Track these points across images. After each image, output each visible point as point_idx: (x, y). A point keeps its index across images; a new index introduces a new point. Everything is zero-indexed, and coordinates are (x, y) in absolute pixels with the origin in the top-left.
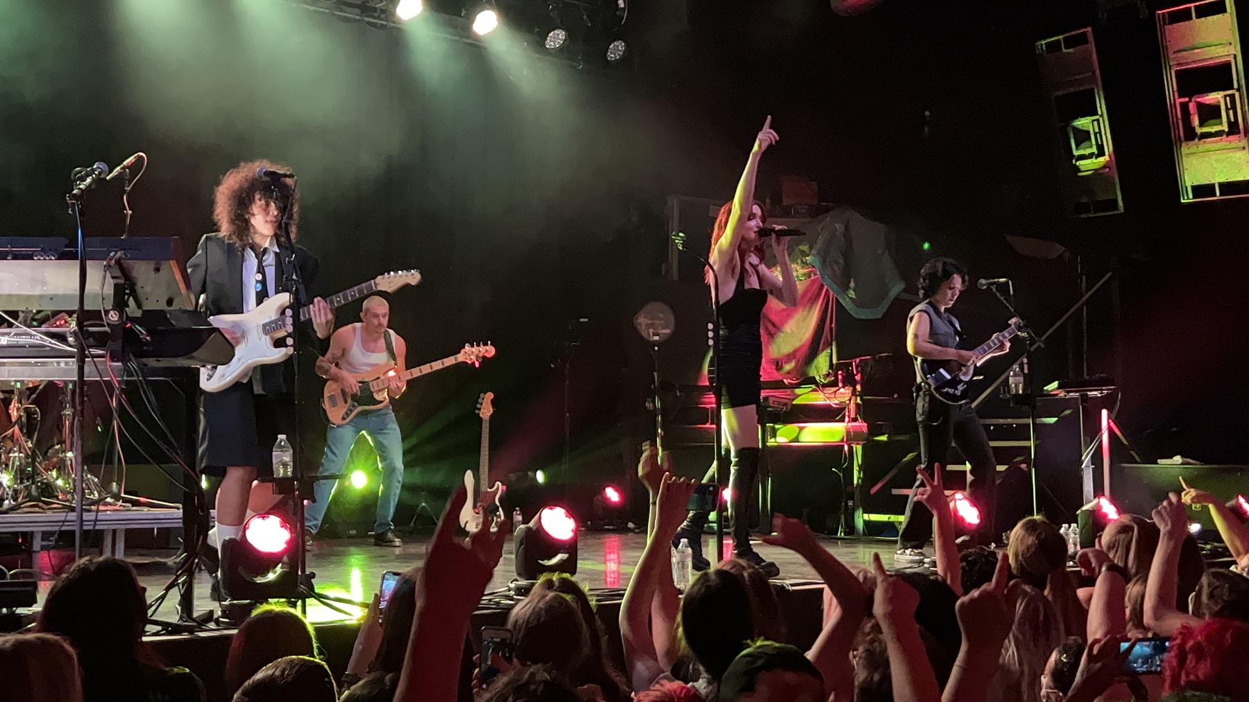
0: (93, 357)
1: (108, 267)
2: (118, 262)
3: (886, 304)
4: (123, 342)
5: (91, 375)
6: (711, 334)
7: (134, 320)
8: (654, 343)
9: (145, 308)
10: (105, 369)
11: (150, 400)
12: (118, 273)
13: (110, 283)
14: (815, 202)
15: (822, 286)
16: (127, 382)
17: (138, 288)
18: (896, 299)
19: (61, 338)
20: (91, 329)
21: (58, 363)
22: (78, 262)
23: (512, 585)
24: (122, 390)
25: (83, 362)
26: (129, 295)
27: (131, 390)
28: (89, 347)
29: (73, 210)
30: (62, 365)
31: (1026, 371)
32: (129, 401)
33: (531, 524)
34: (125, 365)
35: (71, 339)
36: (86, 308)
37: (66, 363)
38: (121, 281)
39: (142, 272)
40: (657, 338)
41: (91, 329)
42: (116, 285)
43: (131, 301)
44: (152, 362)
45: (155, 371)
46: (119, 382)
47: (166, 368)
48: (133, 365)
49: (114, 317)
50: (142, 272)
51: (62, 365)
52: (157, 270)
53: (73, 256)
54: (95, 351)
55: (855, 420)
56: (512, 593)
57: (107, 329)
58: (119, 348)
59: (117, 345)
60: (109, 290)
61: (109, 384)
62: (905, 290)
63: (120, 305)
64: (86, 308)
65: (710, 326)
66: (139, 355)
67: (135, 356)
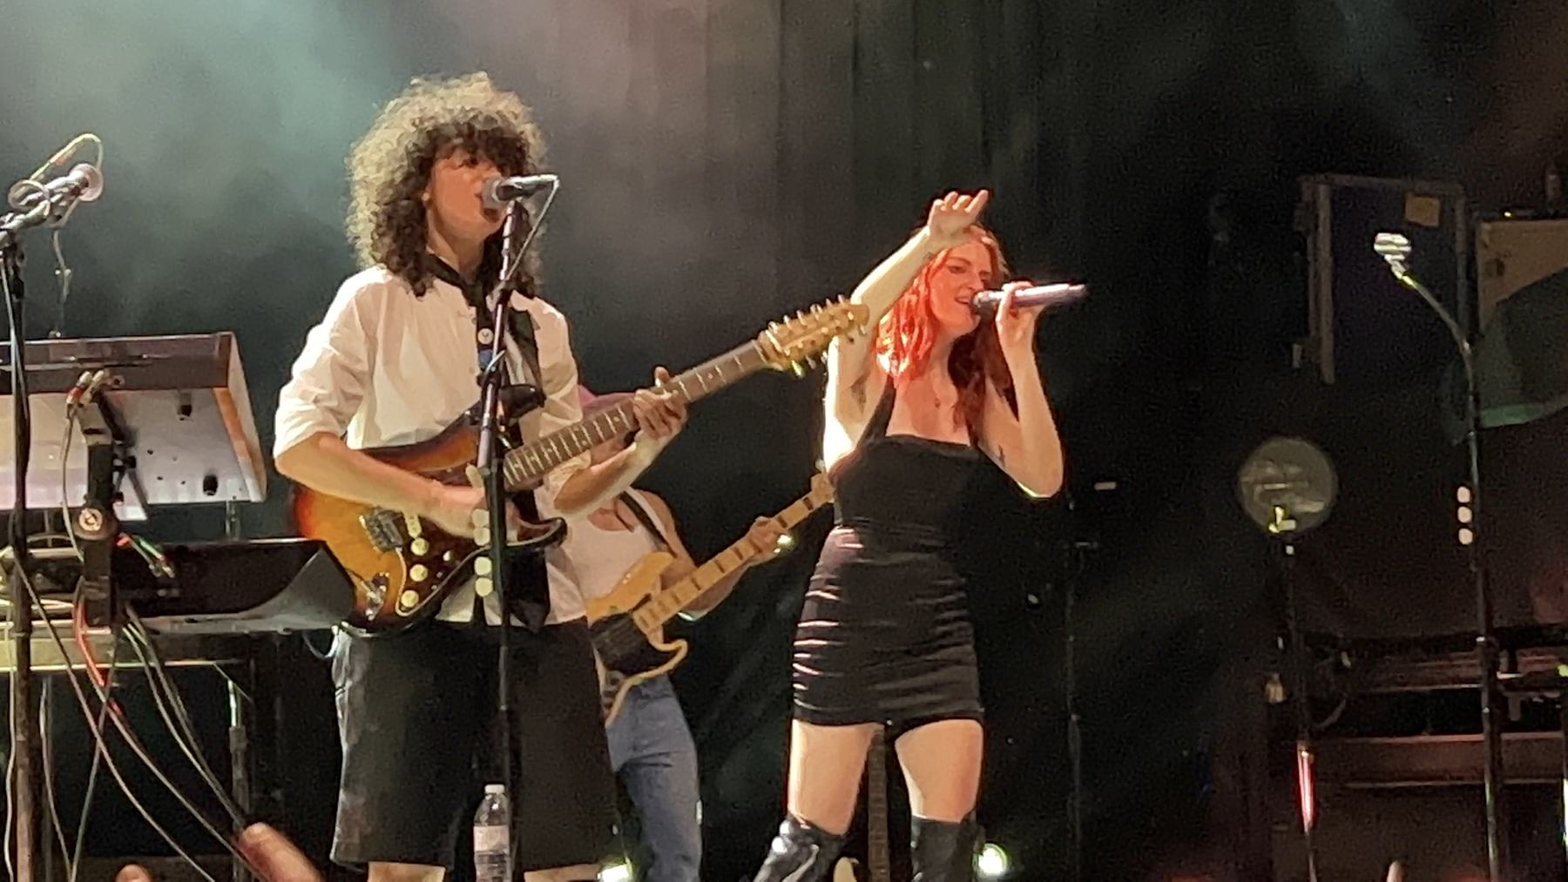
0: (50, 617)
1: (75, 410)
2: (98, 397)
4: (120, 580)
5: (46, 660)
6: (1465, 515)
7: (132, 528)
9: (150, 501)
11: (173, 709)
12: (99, 423)
13: (82, 443)
16: (119, 671)
17: (138, 452)
20: (38, 553)
22: (10, 400)
24: (113, 693)
25: (28, 629)
26: (121, 470)
27: (132, 691)
28: (39, 594)
34: (119, 634)
36: (29, 505)
39: (149, 412)
41: (38, 553)
43: (126, 488)
45: (185, 646)
46: (104, 672)
47: (205, 638)
48: (135, 632)
49: (91, 524)
50: (149, 412)
52: (186, 410)
57: (74, 551)
61: (83, 677)
63: (104, 495)
64: (29, 505)
65: (1463, 495)
66: (148, 609)
67: (141, 615)
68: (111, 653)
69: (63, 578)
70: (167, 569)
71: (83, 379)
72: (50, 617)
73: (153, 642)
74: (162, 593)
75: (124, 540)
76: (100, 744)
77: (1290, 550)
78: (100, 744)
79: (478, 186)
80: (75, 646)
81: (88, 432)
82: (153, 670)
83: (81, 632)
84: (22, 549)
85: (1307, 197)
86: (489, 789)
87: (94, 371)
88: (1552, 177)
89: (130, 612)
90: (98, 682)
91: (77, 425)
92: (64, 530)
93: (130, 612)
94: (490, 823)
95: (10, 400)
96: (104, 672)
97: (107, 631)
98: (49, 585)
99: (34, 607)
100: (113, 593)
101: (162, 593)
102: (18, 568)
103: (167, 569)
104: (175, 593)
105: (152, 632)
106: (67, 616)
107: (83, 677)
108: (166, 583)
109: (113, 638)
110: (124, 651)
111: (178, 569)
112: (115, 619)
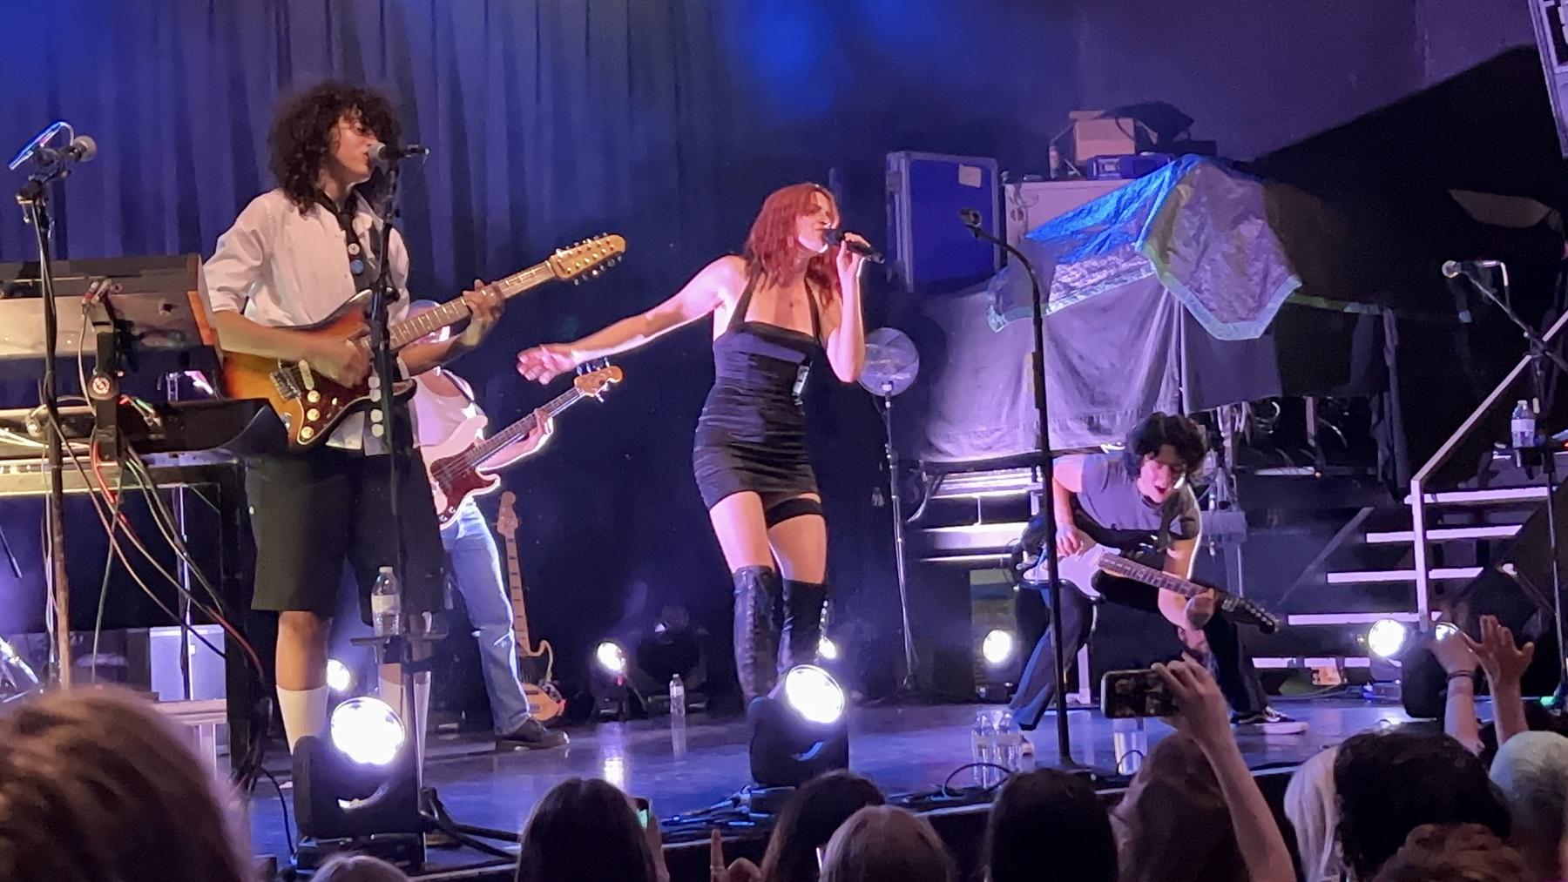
0: (76, 455)
1: (88, 309)
2: (105, 298)
3: (1267, 318)
8: (882, 400)
10: (96, 477)
12: (105, 317)
14: (1129, 148)
15: (1161, 288)
16: (124, 493)
18: (1287, 310)
19: (18, 427)
20: (62, 410)
21: (7, 468)
22: (41, 302)
23: (746, 797)
24: (120, 508)
25: (60, 463)
27: (134, 504)
29: (30, 217)
30: (14, 471)
31: (1537, 410)
32: (129, 524)
33: (771, 696)
35: (32, 428)
37: (23, 469)
38: (109, 330)
40: (887, 388)
41: (62, 410)
42: (100, 337)
44: (162, 460)
48: (135, 464)
51: (14, 471)
53: (31, 292)
54: (78, 446)
55: (1224, 505)
56: (744, 809)
57: (89, 408)
58: (112, 439)
59: (108, 435)
60: (91, 347)
62: (1297, 291)
66: (145, 447)
67: (139, 452)
68: (118, 480)
69: (82, 428)
70: (157, 420)
71: (94, 286)
72: (76, 455)
73: (148, 471)
74: (153, 436)
75: (125, 399)
76: (113, 541)
77: (888, 404)
78: (113, 541)
79: (365, 149)
80: (96, 477)
81: (95, 324)
82: (149, 492)
83: (95, 465)
84: (53, 406)
85: (894, 167)
86: (382, 570)
87: (100, 282)
88: (1053, 154)
89: (130, 450)
90: (110, 501)
91: (89, 322)
92: (82, 394)
93: (130, 450)
94: (384, 592)
95: (41, 302)
96: (113, 493)
97: (115, 464)
98: (70, 433)
99: (65, 448)
100: (118, 438)
101: (153, 436)
102: (52, 419)
103: (157, 420)
104: (161, 436)
105: (146, 464)
106: (86, 454)
107: (99, 496)
108: (155, 429)
109: (119, 470)
110: (127, 476)
111: (164, 420)
112: (120, 454)
